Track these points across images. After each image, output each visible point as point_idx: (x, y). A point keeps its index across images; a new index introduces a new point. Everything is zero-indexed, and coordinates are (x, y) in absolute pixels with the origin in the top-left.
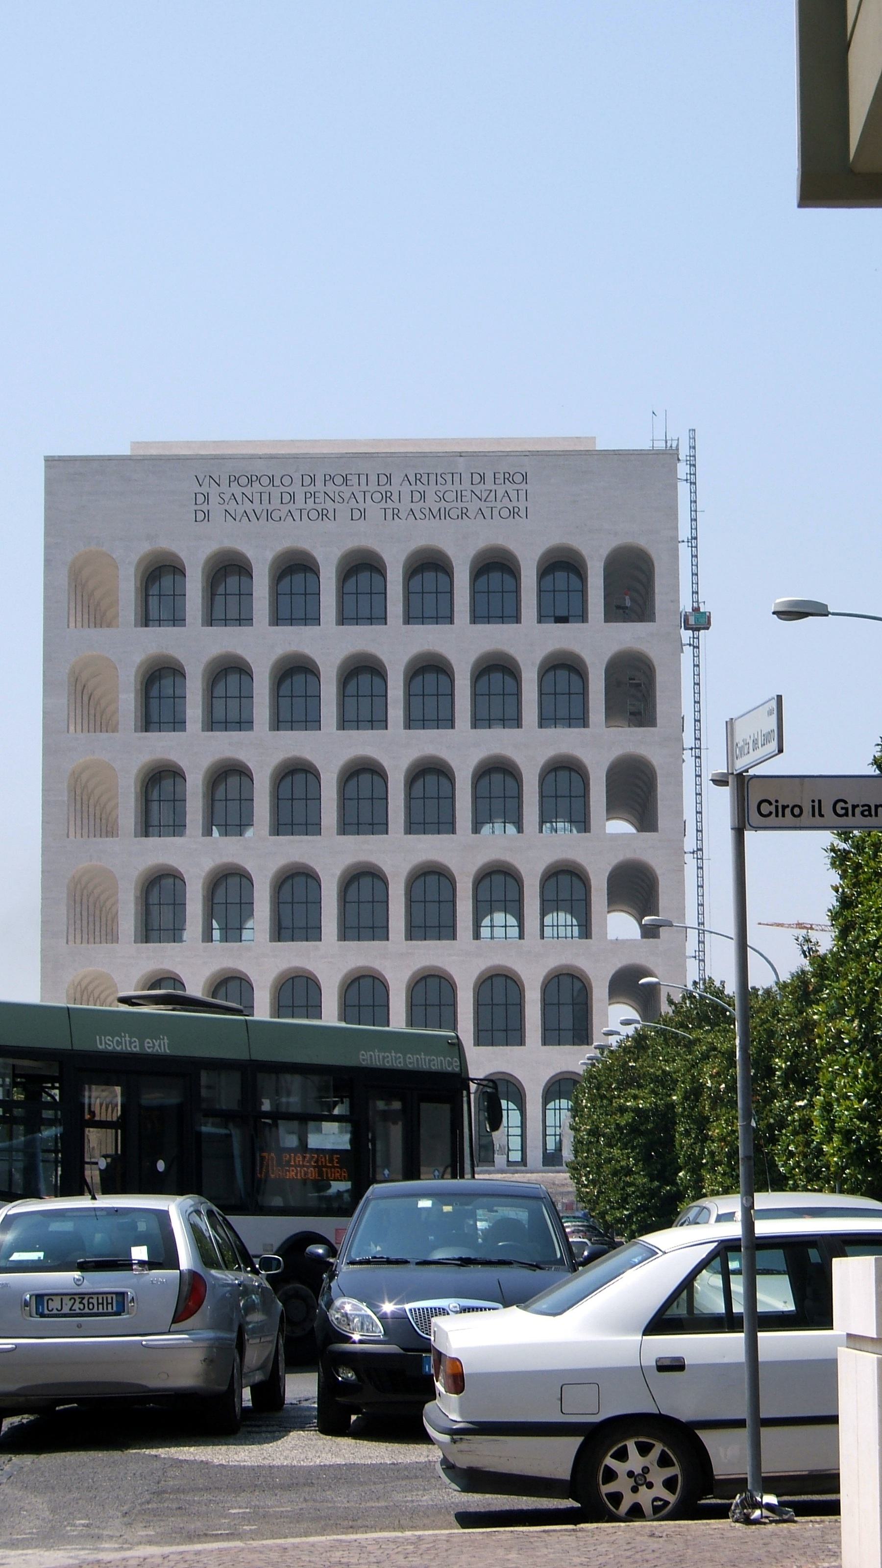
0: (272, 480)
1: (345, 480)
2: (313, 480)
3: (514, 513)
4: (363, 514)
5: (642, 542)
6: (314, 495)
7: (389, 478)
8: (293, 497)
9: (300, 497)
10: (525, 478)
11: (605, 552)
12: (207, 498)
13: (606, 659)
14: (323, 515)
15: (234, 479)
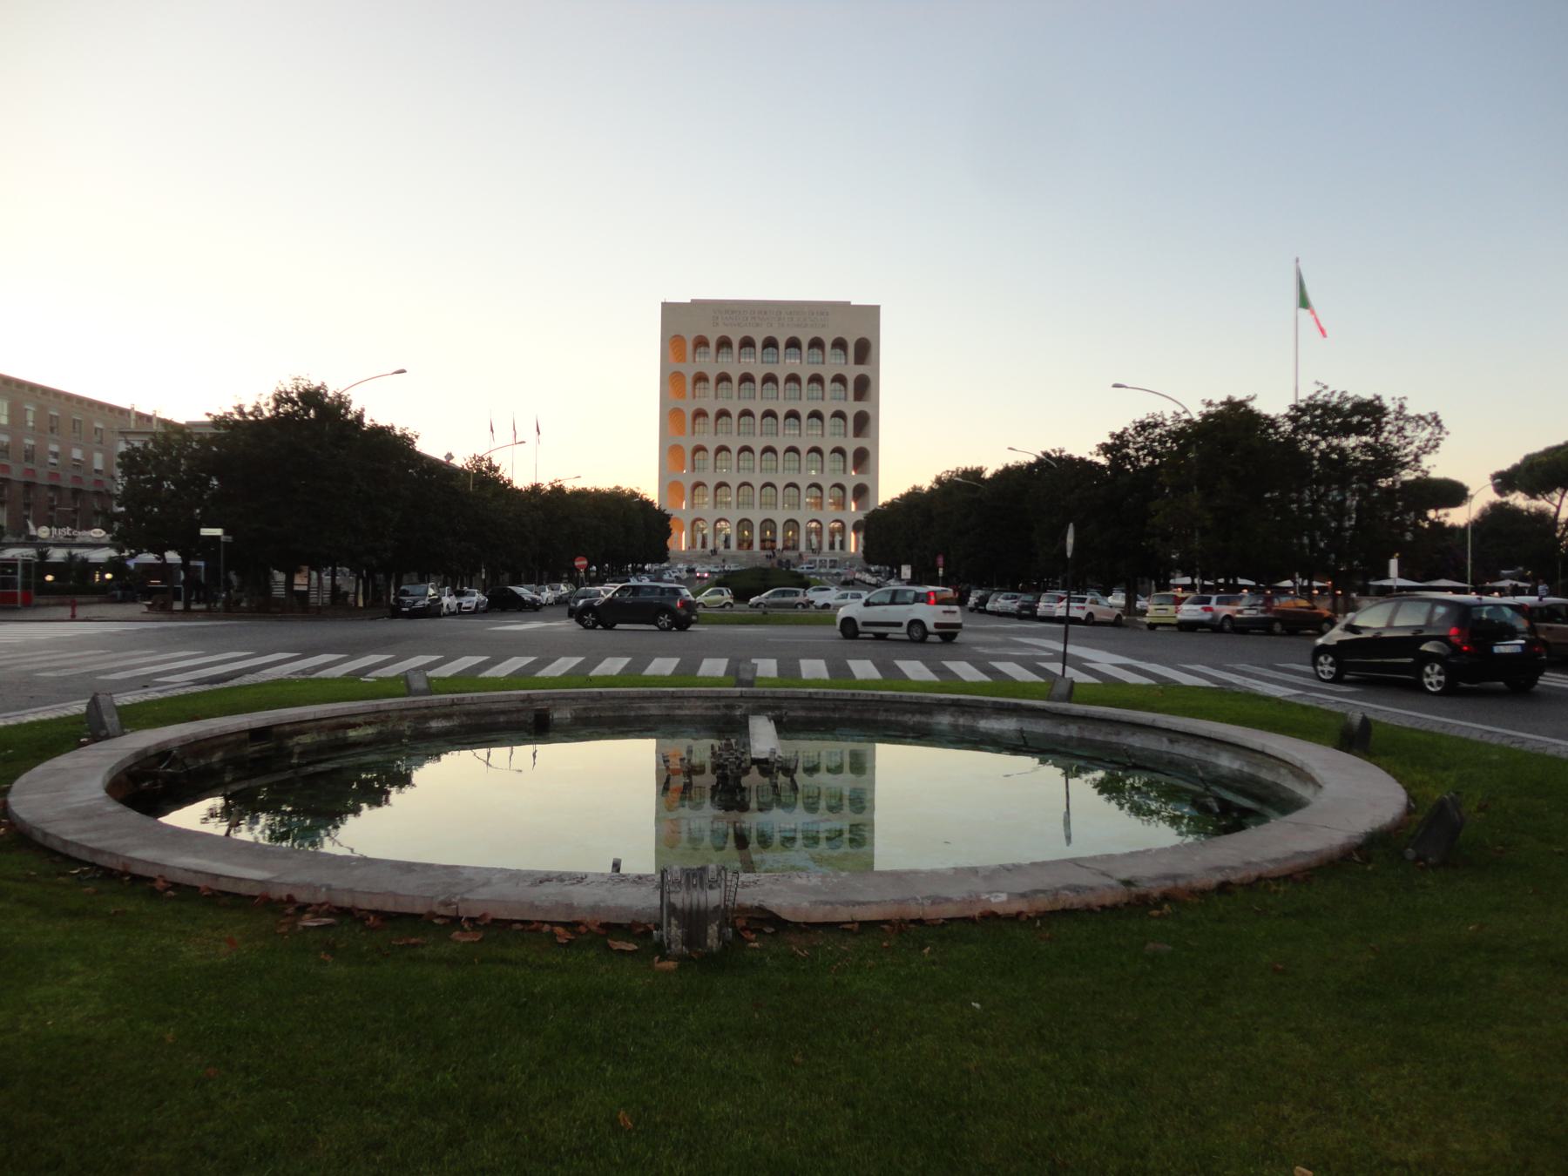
0: (740, 312)
1: (765, 313)
2: (754, 313)
3: (823, 326)
4: (771, 325)
5: (867, 337)
6: (754, 318)
7: (781, 313)
8: (747, 319)
9: (749, 319)
10: (827, 314)
11: (855, 339)
12: (717, 318)
13: (855, 377)
14: (758, 325)
15: (727, 312)
